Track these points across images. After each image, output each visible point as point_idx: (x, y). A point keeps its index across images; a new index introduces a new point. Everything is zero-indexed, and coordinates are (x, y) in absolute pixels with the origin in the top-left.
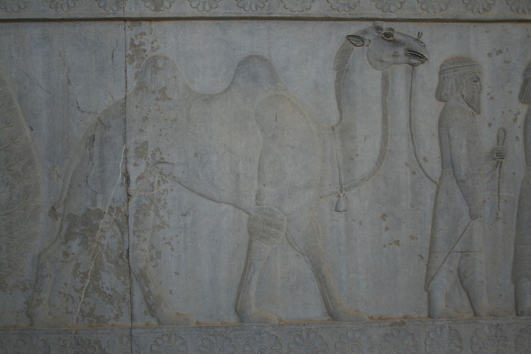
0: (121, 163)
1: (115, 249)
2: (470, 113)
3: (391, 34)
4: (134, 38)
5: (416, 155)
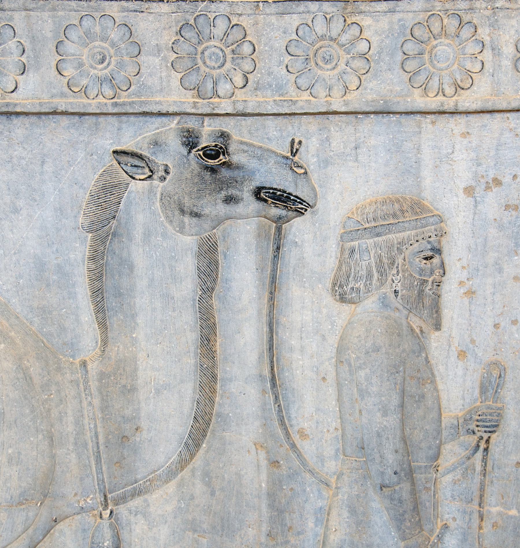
2: (412, 330)
3: (221, 148)
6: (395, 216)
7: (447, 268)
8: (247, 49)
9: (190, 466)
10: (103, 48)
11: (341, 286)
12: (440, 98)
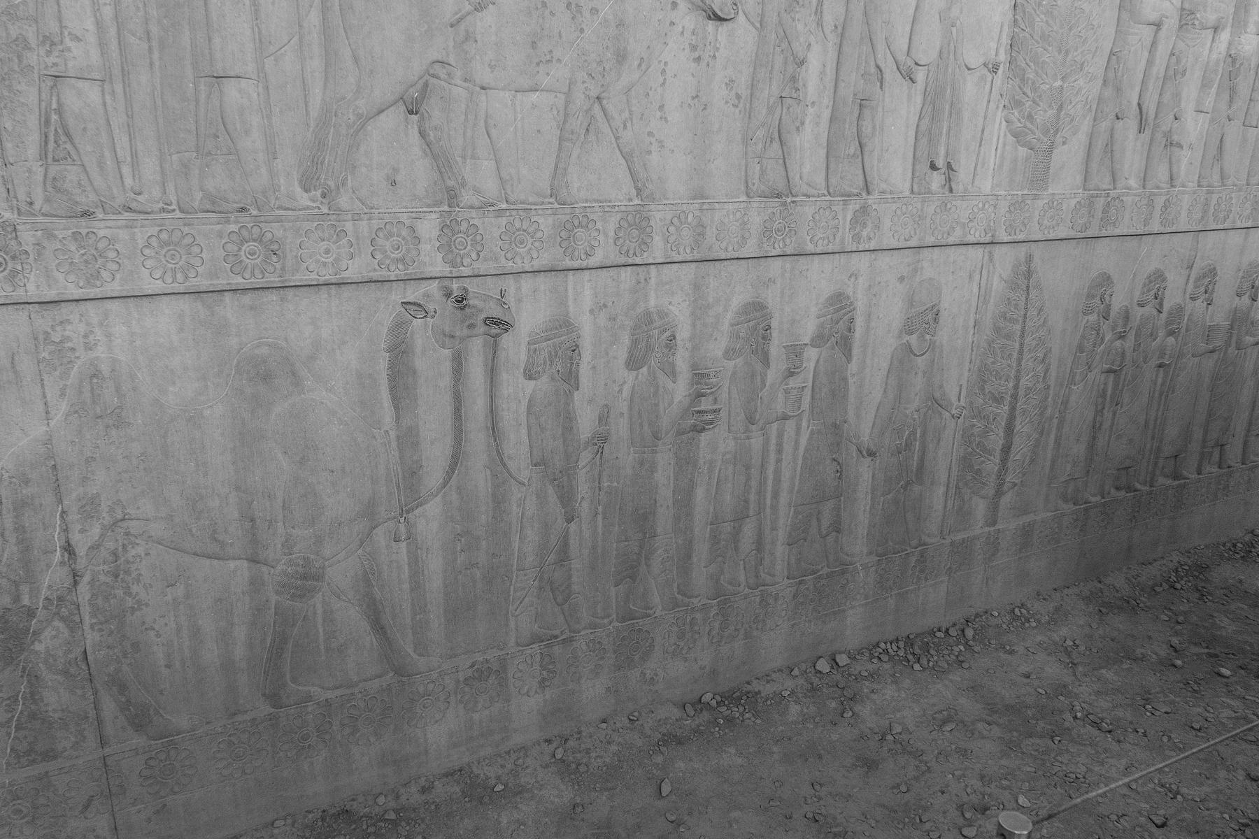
5: (498, 453)
8: (479, 238)
9: (449, 485)
10: (399, 241)
11: (530, 371)
12: (579, 261)
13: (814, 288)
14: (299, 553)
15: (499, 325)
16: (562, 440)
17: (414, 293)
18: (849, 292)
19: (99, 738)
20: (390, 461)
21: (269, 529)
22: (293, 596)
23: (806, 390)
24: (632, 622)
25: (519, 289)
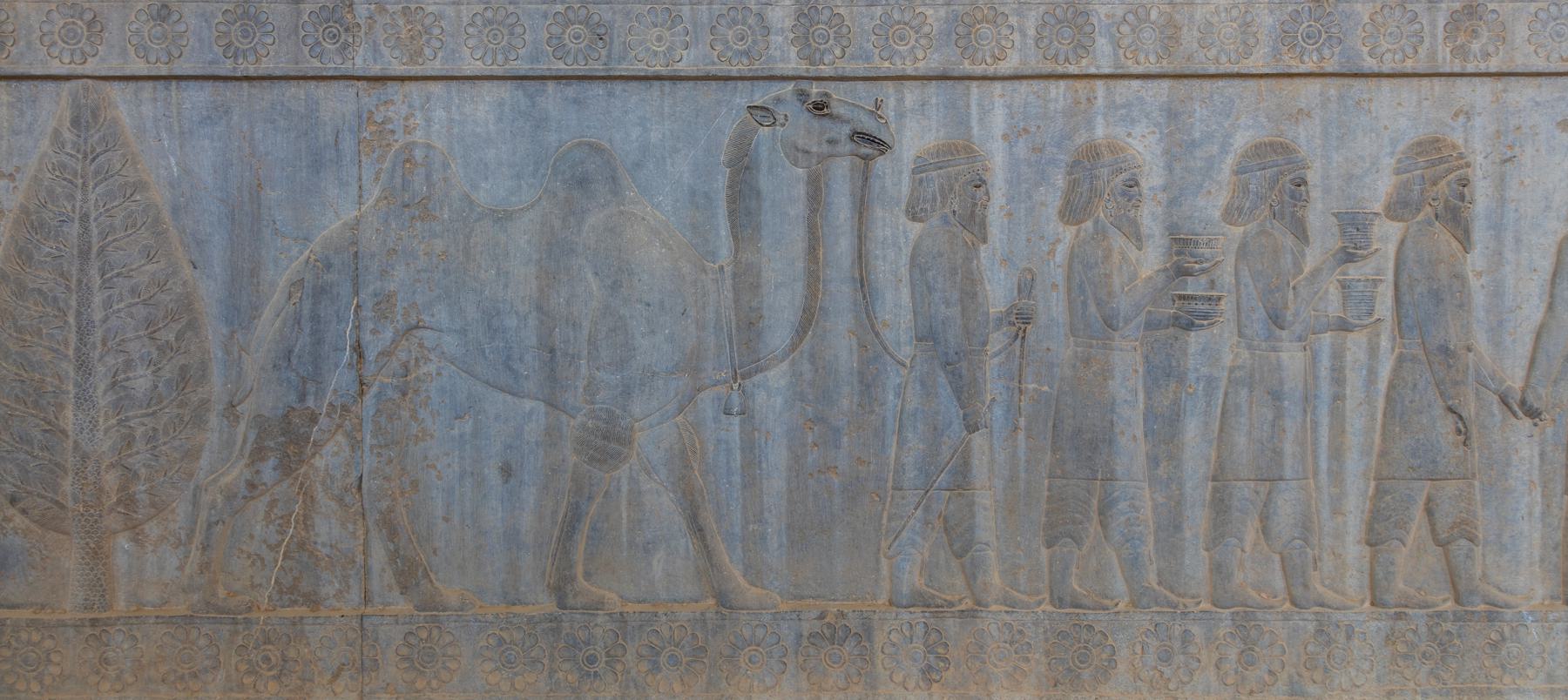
0: (349, 329)
1: (339, 476)
4: (374, 110)
6: (952, 154)
7: (991, 195)
11: (913, 208)
13: (1386, 128)
14: (602, 403)
15: (871, 143)
16: (959, 308)
17: (763, 96)
18: (1457, 138)
19: (363, 591)
20: (722, 303)
21: (570, 365)
22: (592, 460)
23: (1381, 288)
24: (1077, 611)
25: (901, 101)
